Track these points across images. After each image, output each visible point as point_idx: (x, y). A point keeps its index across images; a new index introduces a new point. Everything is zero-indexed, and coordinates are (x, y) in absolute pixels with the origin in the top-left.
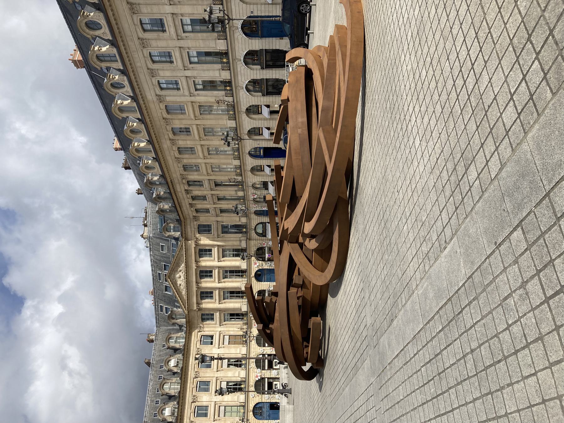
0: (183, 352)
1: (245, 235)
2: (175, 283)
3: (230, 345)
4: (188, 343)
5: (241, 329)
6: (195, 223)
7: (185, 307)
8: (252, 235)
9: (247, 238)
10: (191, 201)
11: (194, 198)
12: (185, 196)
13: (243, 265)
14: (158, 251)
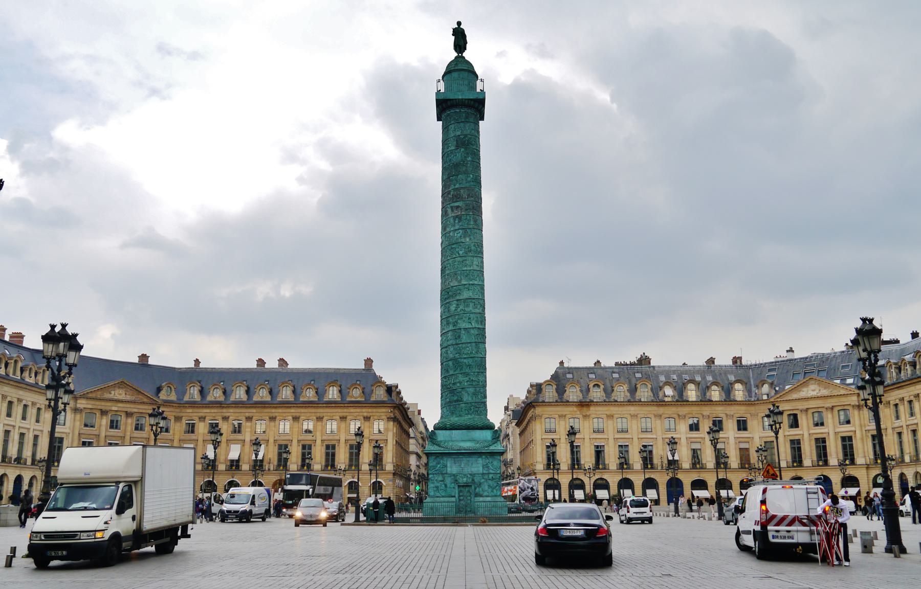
0: (728, 400)
1: (872, 462)
2: (805, 384)
3: (738, 450)
4: (738, 404)
7: (778, 398)
8: (874, 471)
9: (868, 465)
10: (907, 399)
11: (910, 402)
12: (912, 393)
13: (833, 461)
14: (842, 361)
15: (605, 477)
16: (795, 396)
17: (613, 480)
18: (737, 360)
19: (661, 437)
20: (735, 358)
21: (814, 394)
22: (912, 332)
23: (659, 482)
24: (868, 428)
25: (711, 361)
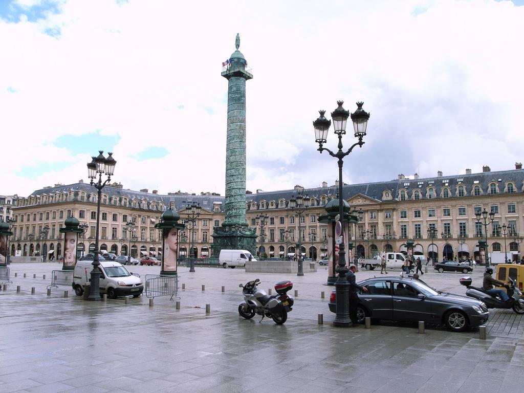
15: (105, 243)
17: (109, 245)
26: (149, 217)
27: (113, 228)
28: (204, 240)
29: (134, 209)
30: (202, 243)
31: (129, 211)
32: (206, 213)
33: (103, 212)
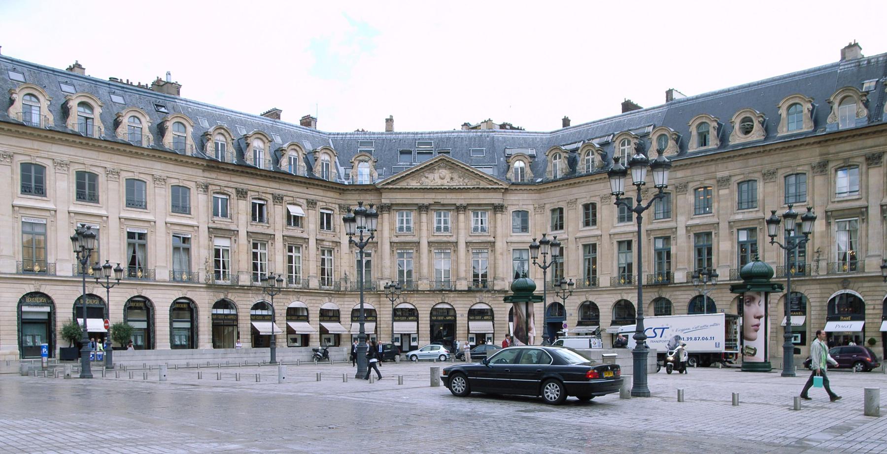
2: (430, 168)
5: (346, 280)
6: (531, 207)
7: (388, 184)
16: (414, 183)
18: (307, 121)
19: (207, 226)
20: (308, 117)
21: (446, 183)
22: (563, 118)
23: (155, 304)
24: (510, 239)
25: (274, 114)
26: (278, 199)
27: (131, 235)
28: (476, 281)
29: (214, 165)
30: (469, 291)
31: (199, 172)
32: (483, 184)
33: (81, 168)
